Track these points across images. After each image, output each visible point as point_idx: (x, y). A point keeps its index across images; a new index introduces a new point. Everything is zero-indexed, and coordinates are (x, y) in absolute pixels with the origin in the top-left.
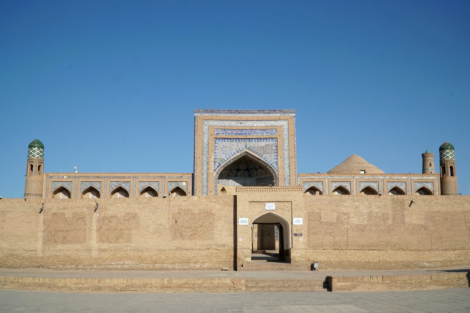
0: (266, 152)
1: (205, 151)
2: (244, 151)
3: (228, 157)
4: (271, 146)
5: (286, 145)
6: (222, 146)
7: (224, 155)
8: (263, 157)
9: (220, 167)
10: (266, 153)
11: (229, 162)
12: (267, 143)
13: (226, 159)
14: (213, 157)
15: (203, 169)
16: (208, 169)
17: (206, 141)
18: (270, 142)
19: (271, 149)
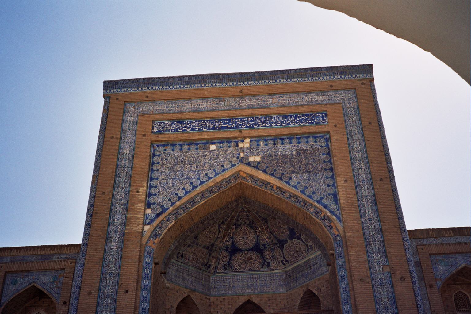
0: (300, 169)
1: (123, 174)
2: (235, 170)
3: (189, 187)
4: (312, 154)
5: (357, 147)
6: (173, 161)
7: (177, 183)
8: (294, 182)
9: (161, 218)
10: (299, 171)
11: (192, 202)
12: (303, 146)
13: (181, 193)
14: (143, 190)
15: (110, 222)
16: (126, 222)
17: (126, 151)
18: (312, 144)
19: (315, 160)
